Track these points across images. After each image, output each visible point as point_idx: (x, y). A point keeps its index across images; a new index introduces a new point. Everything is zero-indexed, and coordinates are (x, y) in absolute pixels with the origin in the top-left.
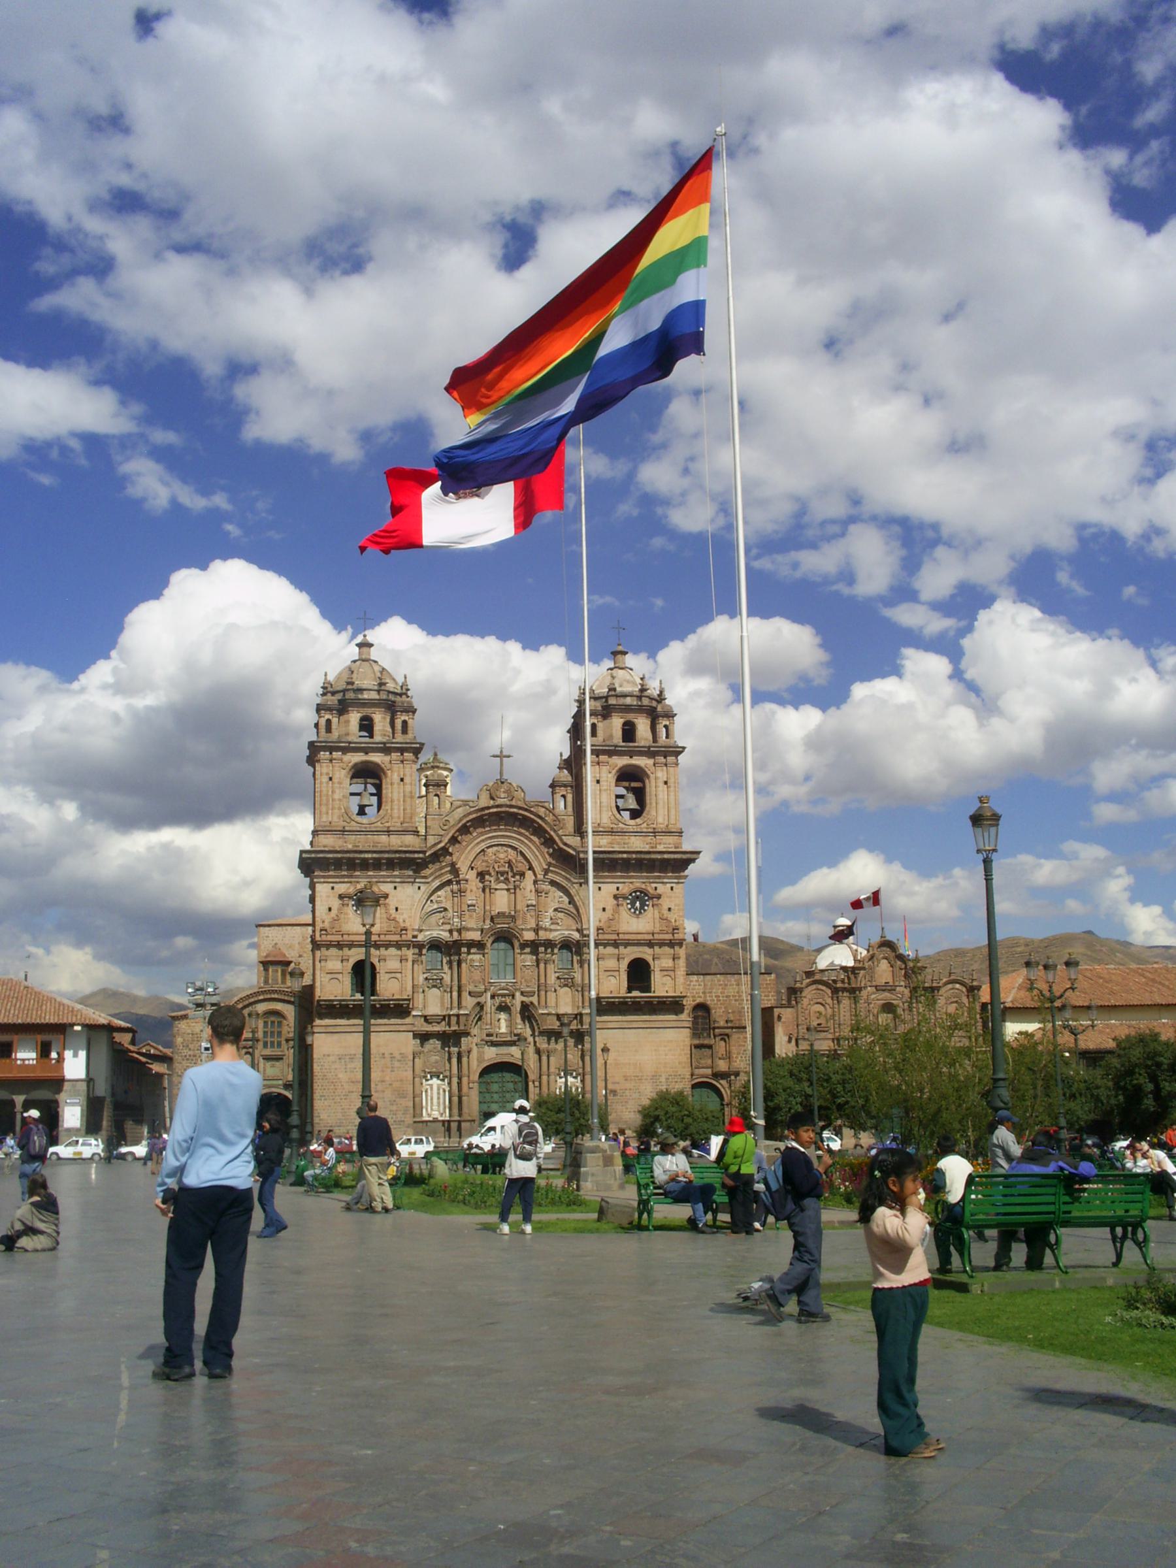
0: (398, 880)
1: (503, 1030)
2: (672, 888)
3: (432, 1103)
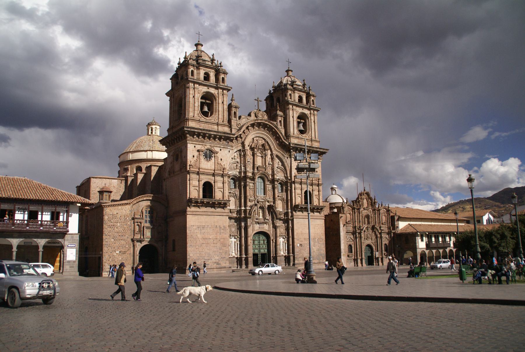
0: (222, 146)
1: (261, 217)
3: (232, 249)
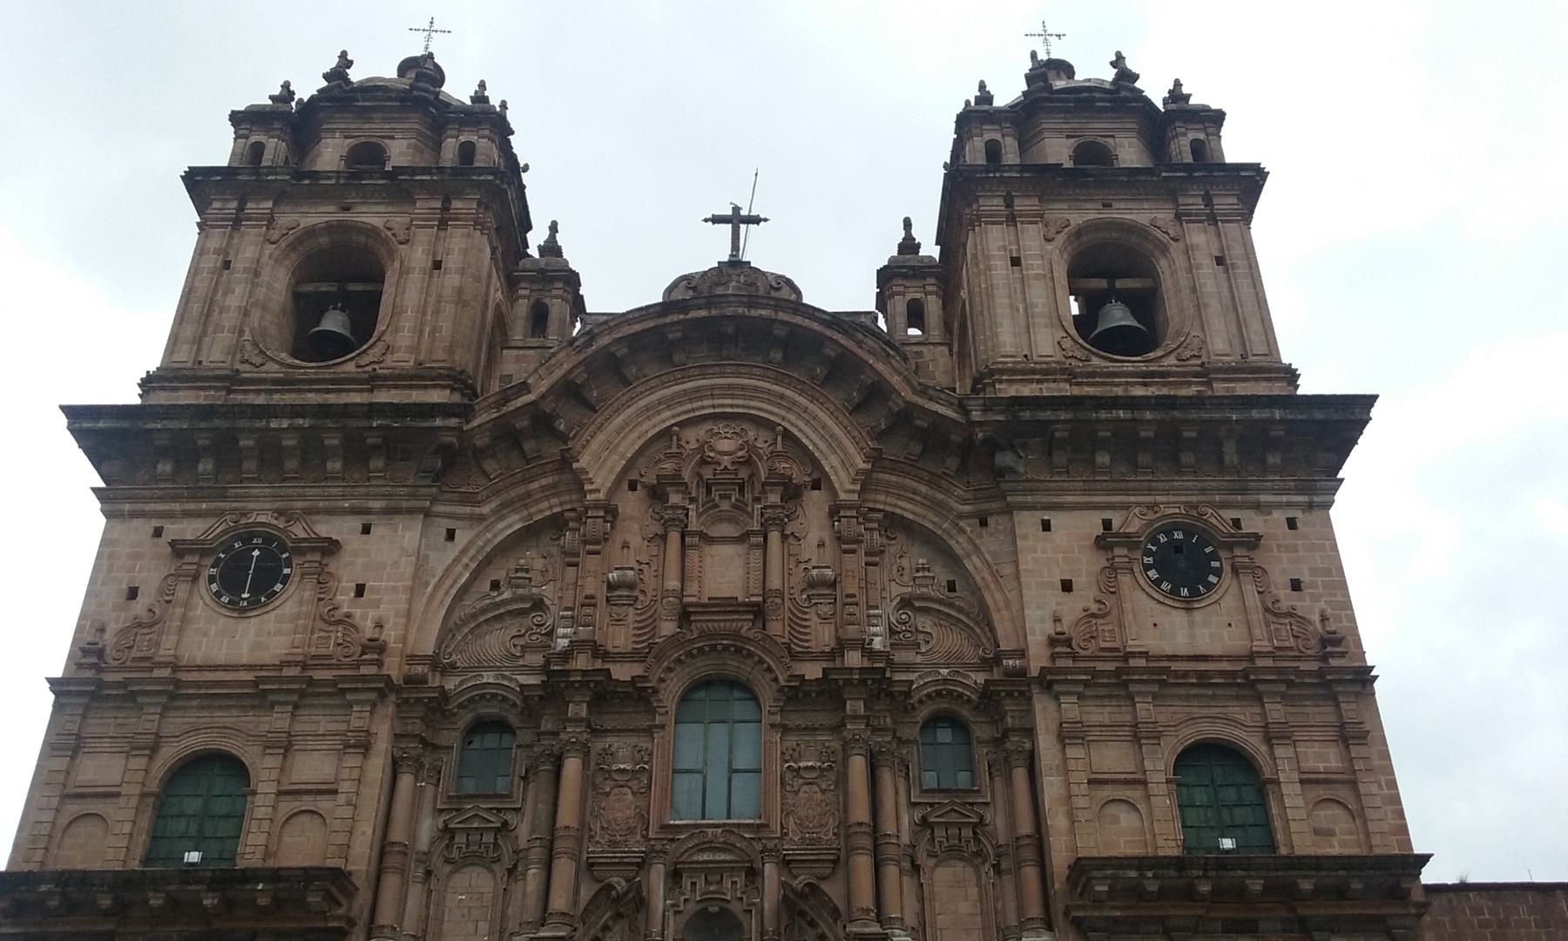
2: (1292, 524)
